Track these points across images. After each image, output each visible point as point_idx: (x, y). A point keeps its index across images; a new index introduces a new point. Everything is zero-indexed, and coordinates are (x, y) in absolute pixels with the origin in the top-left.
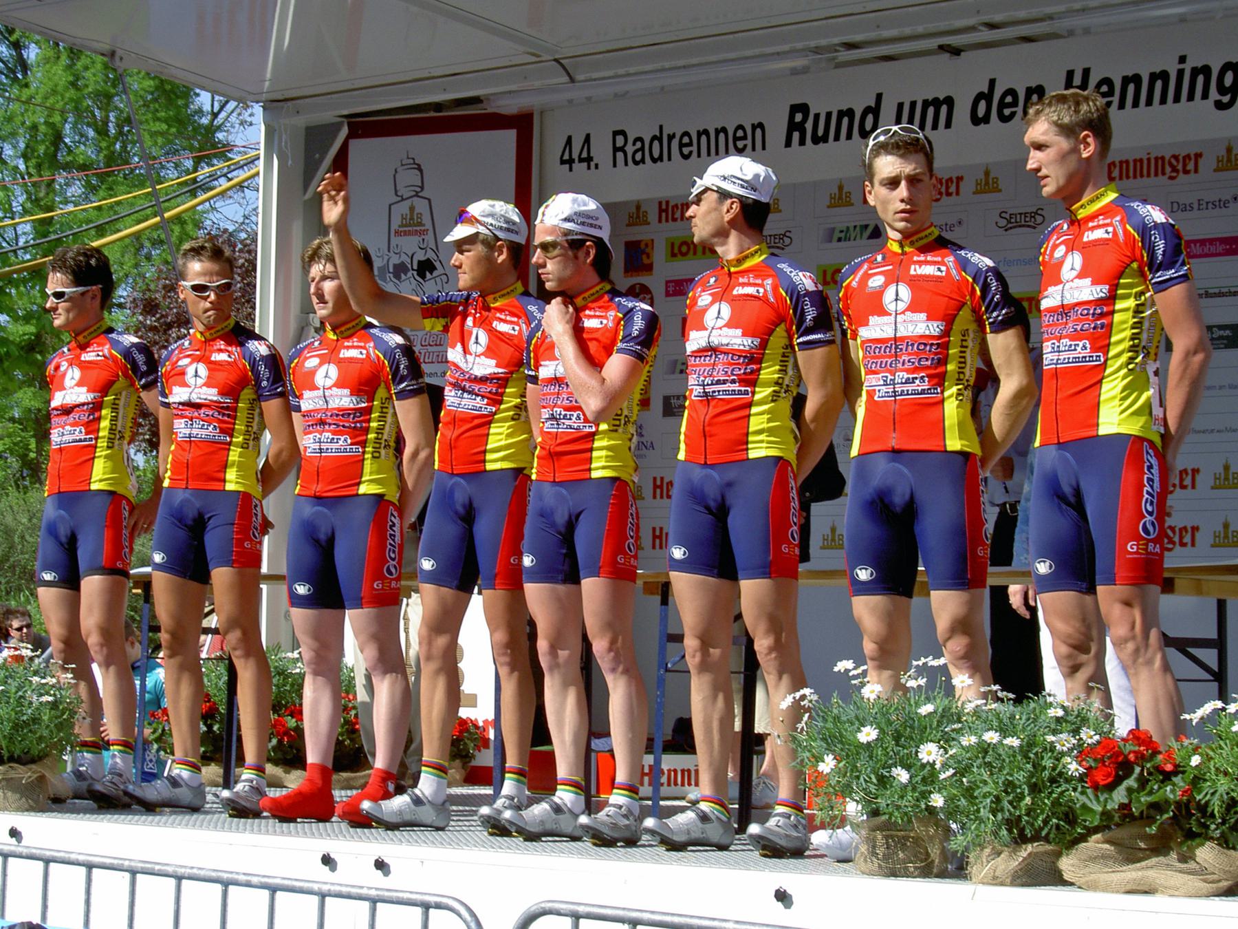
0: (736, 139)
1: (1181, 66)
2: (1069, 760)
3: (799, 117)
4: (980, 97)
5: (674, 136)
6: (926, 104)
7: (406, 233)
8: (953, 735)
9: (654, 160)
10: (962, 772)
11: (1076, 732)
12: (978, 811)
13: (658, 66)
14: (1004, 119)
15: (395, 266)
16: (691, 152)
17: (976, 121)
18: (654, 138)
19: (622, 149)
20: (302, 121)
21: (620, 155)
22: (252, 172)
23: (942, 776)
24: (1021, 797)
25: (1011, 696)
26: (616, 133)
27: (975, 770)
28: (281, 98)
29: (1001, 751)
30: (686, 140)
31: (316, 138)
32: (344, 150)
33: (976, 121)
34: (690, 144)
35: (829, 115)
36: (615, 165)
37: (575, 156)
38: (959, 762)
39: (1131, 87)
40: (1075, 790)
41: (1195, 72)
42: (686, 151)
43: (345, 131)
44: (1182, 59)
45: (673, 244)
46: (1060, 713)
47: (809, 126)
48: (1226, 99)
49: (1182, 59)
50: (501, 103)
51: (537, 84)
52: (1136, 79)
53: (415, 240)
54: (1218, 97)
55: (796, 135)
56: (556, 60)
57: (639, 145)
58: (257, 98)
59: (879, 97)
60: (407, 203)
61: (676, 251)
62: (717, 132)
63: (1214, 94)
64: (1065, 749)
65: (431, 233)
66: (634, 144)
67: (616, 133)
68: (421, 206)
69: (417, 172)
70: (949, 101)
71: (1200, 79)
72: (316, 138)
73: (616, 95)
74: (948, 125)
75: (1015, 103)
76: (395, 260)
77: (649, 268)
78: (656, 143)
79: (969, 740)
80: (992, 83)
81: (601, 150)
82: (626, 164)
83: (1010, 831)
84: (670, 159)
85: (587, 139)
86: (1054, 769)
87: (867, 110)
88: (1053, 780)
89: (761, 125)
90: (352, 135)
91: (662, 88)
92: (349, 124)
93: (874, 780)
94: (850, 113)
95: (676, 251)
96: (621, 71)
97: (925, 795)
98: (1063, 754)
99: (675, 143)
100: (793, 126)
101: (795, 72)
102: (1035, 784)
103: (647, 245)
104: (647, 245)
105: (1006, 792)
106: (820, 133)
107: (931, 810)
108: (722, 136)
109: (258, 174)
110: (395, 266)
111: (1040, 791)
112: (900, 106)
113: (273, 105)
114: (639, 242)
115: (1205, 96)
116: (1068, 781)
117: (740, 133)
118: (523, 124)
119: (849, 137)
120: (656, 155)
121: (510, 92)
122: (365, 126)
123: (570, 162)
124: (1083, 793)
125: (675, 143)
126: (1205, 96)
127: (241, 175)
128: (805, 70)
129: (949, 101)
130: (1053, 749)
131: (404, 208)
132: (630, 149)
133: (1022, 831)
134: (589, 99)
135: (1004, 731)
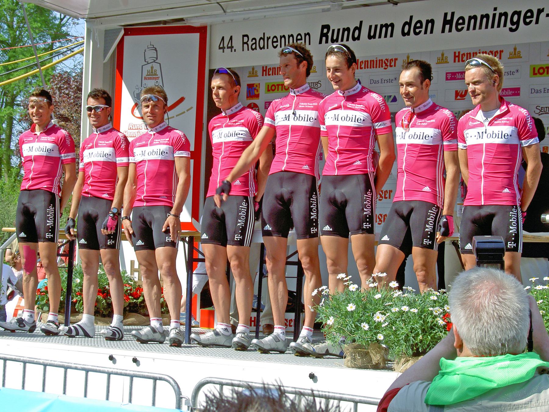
1: (495, 12)
2: (439, 319)
3: (325, 31)
4: (406, 23)
6: (382, 26)
7: (149, 79)
8: (389, 307)
9: (261, 48)
10: (393, 323)
11: (442, 306)
12: (399, 340)
13: (263, 7)
14: (416, 34)
16: (277, 45)
17: (404, 34)
18: (261, 38)
19: (246, 43)
20: (103, 27)
21: (245, 46)
22: (81, 49)
23: (383, 326)
24: (417, 335)
25: (414, 290)
27: (398, 322)
28: (94, 17)
29: (409, 314)
30: (275, 40)
31: (109, 34)
32: (122, 40)
33: (404, 34)
34: (277, 42)
35: (339, 30)
36: (243, 50)
37: (226, 45)
38: (391, 319)
39: (473, 21)
40: (441, 332)
41: (501, 15)
42: (275, 44)
43: (123, 32)
44: (495, 9)
45: (268, 86)
46: (435, 298)
47: (330, 35)
48: (514, 27)
49: (495, 9)
50: (192, 21)
51: (209, 13)
52: (475, 17)
54: (511, 26)
55: (324, 39)
56: (218, 3)
57: (254, 41)
58: (83, 16)
59: (361, 22)
60: (150, 65)
61: (270, 89)
62: (289, 37)
63: (509, 25)
64: (437, 314)
65: (160, 78)
67: (244, 36)
68: (156, 67)
70: (392, 25)
71: (503, 18)
72: (109, 34)
73: (244, 19)
75: (421, 27)
77: (257, 96)
78: (262, 41)
79: (395, 309)
80: (411, 17)
81: (237, 43)
82: (248, 50)
83: (412, 349)
84: (268, 48)
85: (231, 37)
86: (432, 322)
87: (356, 28)
88: (432, 328)
89: (308, 34)
90: (126, 34)
91: (265, 16)
92: (125, 29)
93: (353, 326)
94: (348, 29)
95: (270, 89)
96: (246, 9)
97: (376, 334)
98: (436, 317)
100: (323, 35)
101: (324, 11)
102: (424, 329)
103: (257, 86)
104: (257, 86)
105: (411, 332)
106: (335, 38)
107: (377, 340)
108: (291, 38)
109: (83, 50)
111: (426, 332)
112: (371, 27)
113: (90, 20)
114: (253, 84)
115: (505, 25)
116: (438, 328)
117: (299, 37)
118: (202, 31)
120: (262, 46)
121: (197, 17)
122: (131, 30)
123: (223, 48)
124: (445, 333)
126: (505, 25)
127: (76, 50)
128: (328, 10)
129: (392, 25)
130: (431, 313)
131: (148, 67)
132: (250, 43)
133: (418, 349)
134: (232, 20)
135: (410, 305)
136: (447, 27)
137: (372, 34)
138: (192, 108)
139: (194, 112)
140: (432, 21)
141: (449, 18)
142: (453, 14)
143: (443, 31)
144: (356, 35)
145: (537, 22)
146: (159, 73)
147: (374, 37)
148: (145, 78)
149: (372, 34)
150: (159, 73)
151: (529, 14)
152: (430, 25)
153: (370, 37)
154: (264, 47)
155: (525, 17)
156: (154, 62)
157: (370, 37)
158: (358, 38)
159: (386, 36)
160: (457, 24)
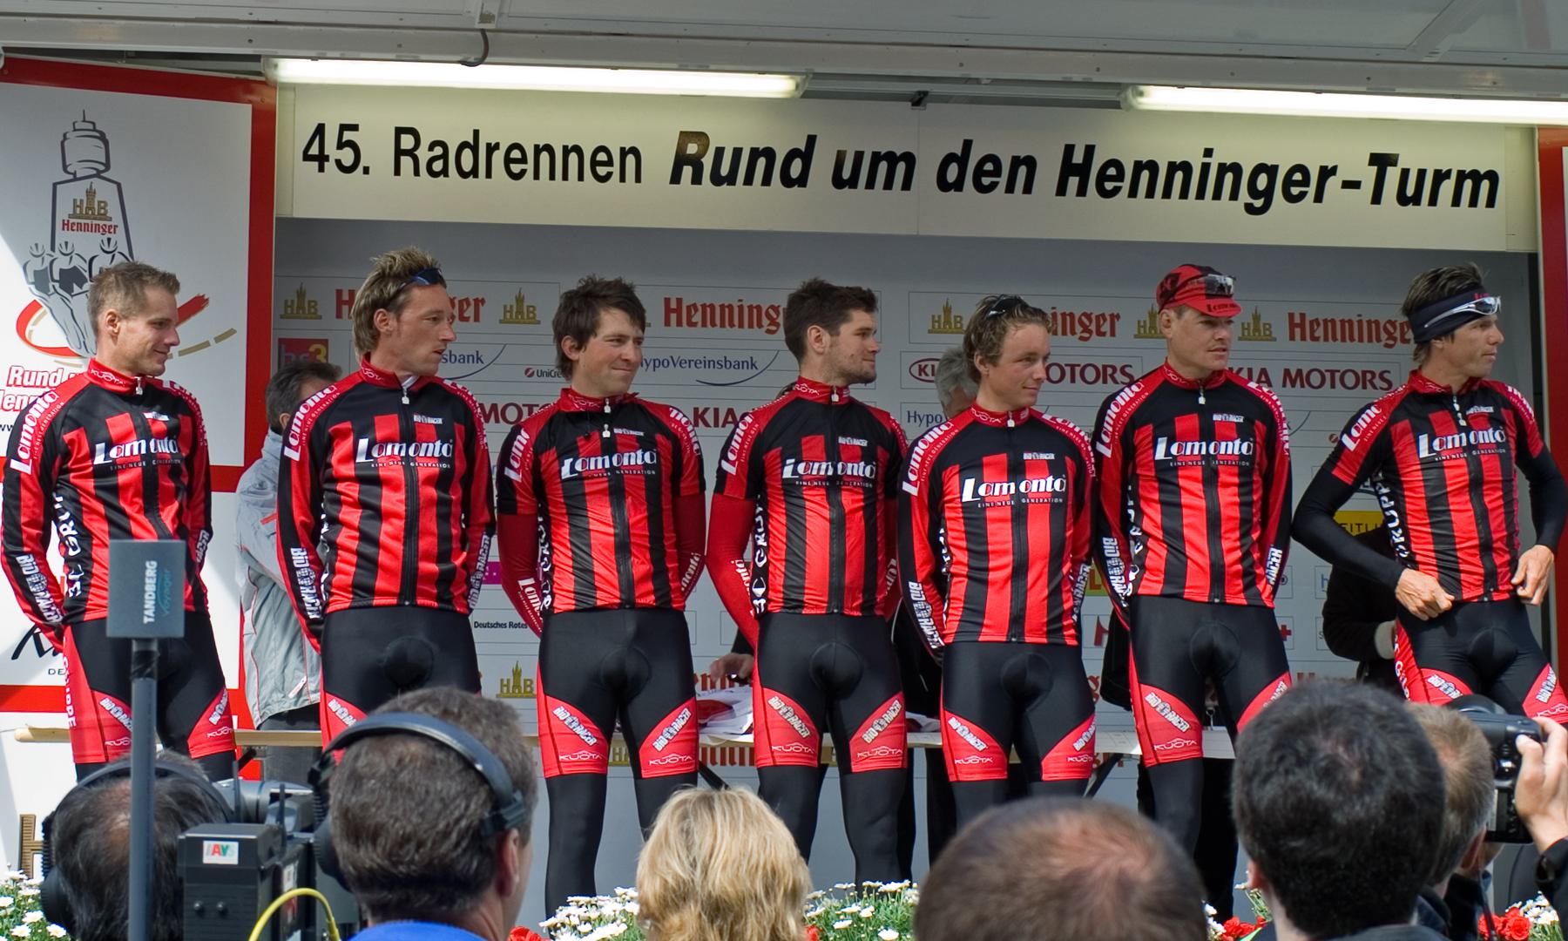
0: (595, 163)
1: (1207, 160)
4: (949, 159)
5: (497, 146)
6: (877, 158)
7: (86, 228)
15: (62, 271)
17: (943, 185)
18: (464, 145)
19: (410, 152)
21: (406, 162)
26: (400, 131)
30: (516, 154)
33: (943, 185)
34: (524, 160)
36: (397, 172)
39: (1145, 175)
41: (1223, 169)
44: (1208, 153)
47: (708, 161)
48: (1259, 203)
49: (1208, 153)
53: (98, 237)
54: (1250, 200)
57: (438, 151)
59: (811, 140)
62: (566, 151)
65: (121, 230)
66: (431, 148)
67: (400, 131)
68: (105, 192)
69: (100, 144)
70: (909, 159)
71: (1229, 177)
74: (907, 185)
75: (997, 172)
76: (62, 263)
80: (967, 145)
81: (377, 147)
84: (489, 175)
87: (792, 155)
89: (634, 151)
94: (769, 154)
99: (498, 157)
100: (681, 160)
108: (573, 157)
110: (62, 271)
115: (1234, 196)
117: (602, 157)
119: (766, 181)
125: (498, 157)
126: (1234, 196)
129: (909, 159)
131: (78, 191)
132: (424, 154)
136: (1073, 182)
137: (846, 174)
138: (231, 332)
139: (239, 343)
140: (1030, 163)
141: (1078, 158)
142: (1090, 150)
143: (1061, 190)
144: (796, 168)
145: (1319, 198)
146: (114, 211)
147: (852, 183)
148: (65, 225)
149: (846, 174)
150: (114, 211)
151: (1298, 176)
152: (1023, 170)
153: (838, 182)
154: (474, 172)
155: (1288, 183)
156: (98, 175)
157: (838, 182)
158: (802, 181)
159: (888, 185)
160: (1102, 178)
